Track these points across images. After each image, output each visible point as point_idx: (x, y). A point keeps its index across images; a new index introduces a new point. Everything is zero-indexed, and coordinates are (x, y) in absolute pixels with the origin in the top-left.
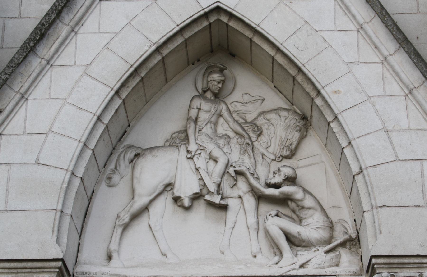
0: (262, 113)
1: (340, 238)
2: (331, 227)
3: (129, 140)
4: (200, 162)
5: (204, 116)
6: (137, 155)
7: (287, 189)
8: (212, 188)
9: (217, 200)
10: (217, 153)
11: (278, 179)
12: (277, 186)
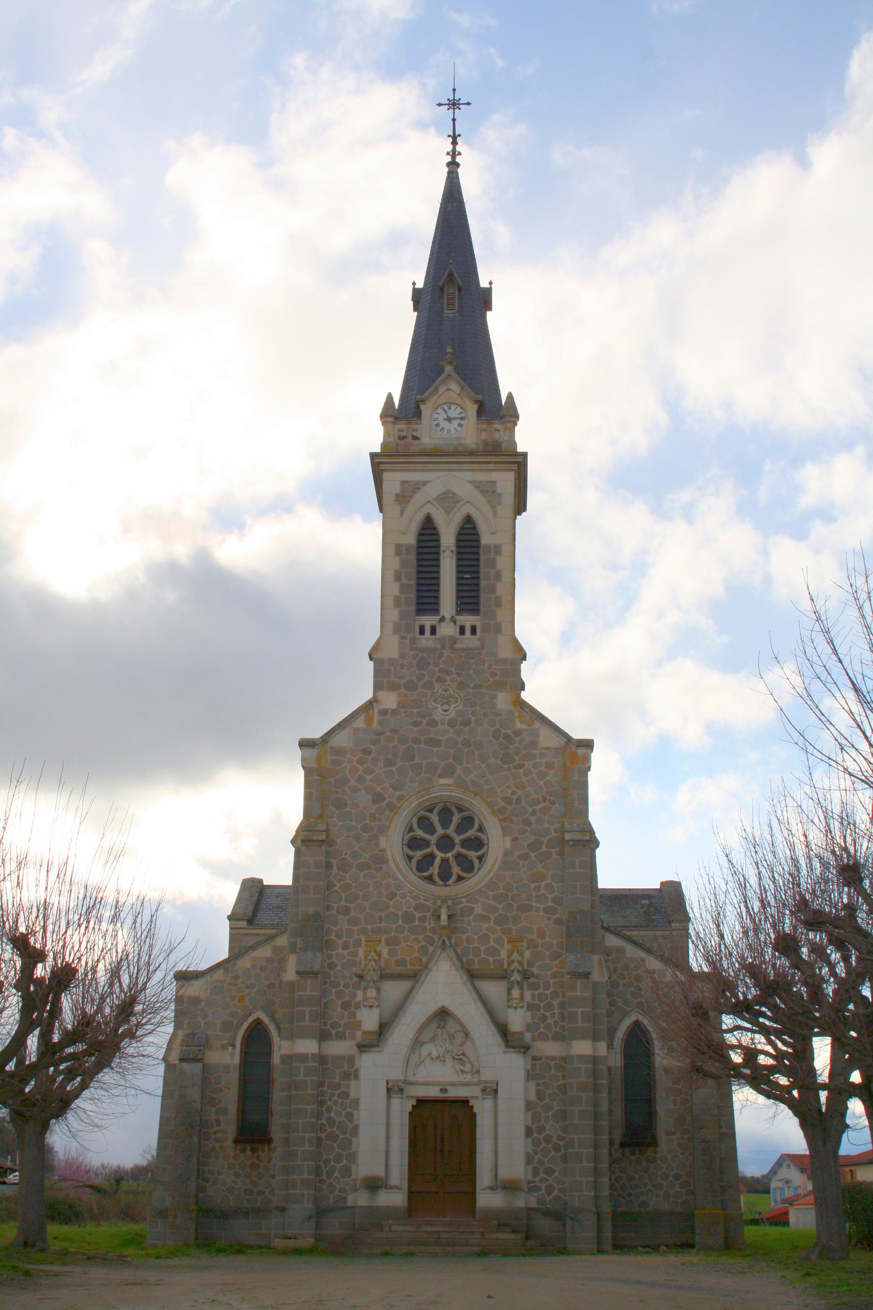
0: (456, 1032)
1: (475, 1071)
2: (473, 1067)
3: (419, 1040)
4: (438, 1048)
5: (439, 1034)
6: (421, 1045)
7: (461, 1057)
8: (441, 1055)
9: (442, 1059)
10: (443, 1045)
11: (458, 1054)
12: (458, 1055)
